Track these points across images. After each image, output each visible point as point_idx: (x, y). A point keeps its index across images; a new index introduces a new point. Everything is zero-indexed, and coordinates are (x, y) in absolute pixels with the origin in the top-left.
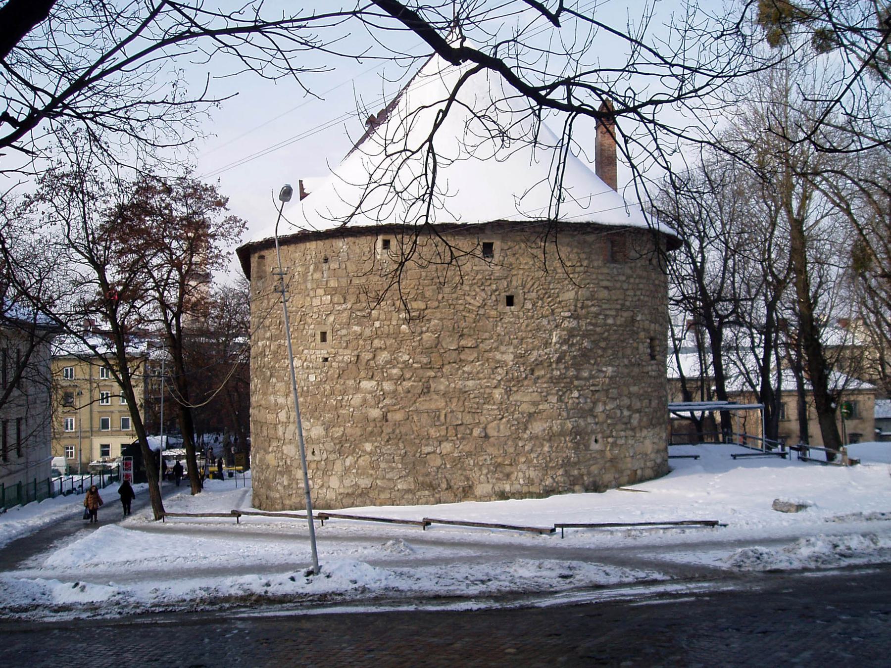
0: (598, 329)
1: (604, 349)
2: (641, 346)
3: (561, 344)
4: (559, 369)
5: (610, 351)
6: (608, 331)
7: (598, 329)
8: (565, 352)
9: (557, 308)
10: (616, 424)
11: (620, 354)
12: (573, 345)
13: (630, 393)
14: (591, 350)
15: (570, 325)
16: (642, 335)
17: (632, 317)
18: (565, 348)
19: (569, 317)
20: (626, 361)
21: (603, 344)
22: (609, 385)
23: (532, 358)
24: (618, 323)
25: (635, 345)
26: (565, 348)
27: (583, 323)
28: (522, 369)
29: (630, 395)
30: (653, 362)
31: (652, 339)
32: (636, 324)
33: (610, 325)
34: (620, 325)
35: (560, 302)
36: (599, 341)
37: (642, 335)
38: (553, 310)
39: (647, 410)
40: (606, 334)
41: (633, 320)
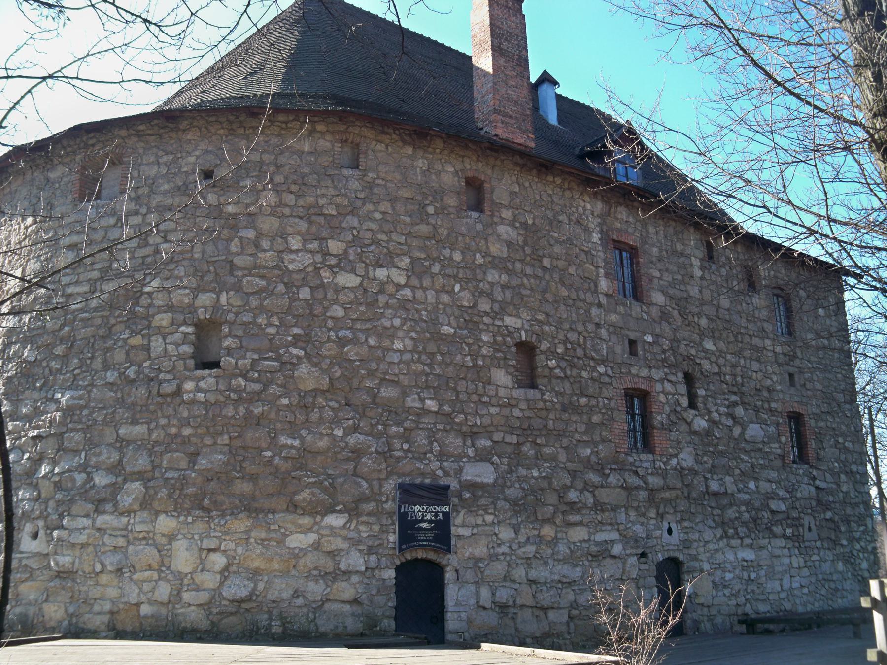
1: (65, 358)
2: (157, 345)
10: (72, 501)
11: (98, 364)
13: (119, 440)
16: (163, 320)
20: (111, 376)
22: (63, 423)
25: (137, 341)
27: (26, 318)
29: (122, 444)
32: (144, 301)
34: (96, 309)
36: (54, 346)
37: (163, 320)
39: (169, 475)
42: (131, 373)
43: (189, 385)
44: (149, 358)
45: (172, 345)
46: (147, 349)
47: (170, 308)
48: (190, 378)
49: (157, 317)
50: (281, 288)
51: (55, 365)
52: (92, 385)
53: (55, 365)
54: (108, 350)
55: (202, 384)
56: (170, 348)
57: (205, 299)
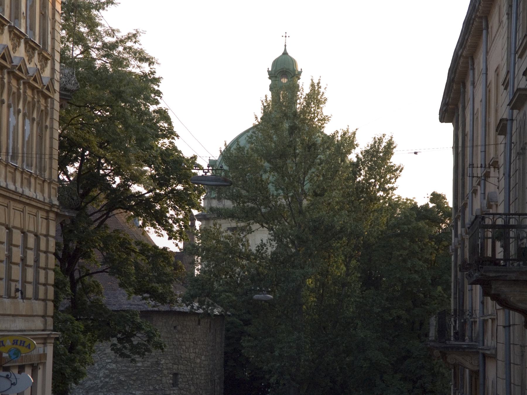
0: (130, 369)
2: (164, 380)
3: (105, 378)
4: (103, 392)
5: (139, 382)
6: (137, 370)
7: (130, 369)
8: (107, 382)
9: (104, 357)
12: (112, 378)
14: (125, 381)
15: (111, 367)
16: (166, 372)
17: (156, 362)
18: (107, 380)
19: (111, 362)
20: (151, 388)
21: (134, 378)
23: (87, 385)
24: (146, 365)
25: (158, 378)
26: (107, 380)
28: (81, 391)
30: (174, 388)
31: (175, 375)
33: (138, 367)
35: (105, 354)
37: (166, 372)
38: (100, 358)
40: (136, 372)
41: (158, 363)
42: (157, 387)
43: (172, 392)
44: (162, 383)
45: (168, 380)
46: (161, 380)
47: (167, 369)
48: (171, 390)
49: (164, 371)
50: (189, 364)
51: (132, 382)
52: (145, 390)
53: (132, 382)
54: (150, 380)
55: (175, 392)
56: (168, 381)
57: (175, 367)
